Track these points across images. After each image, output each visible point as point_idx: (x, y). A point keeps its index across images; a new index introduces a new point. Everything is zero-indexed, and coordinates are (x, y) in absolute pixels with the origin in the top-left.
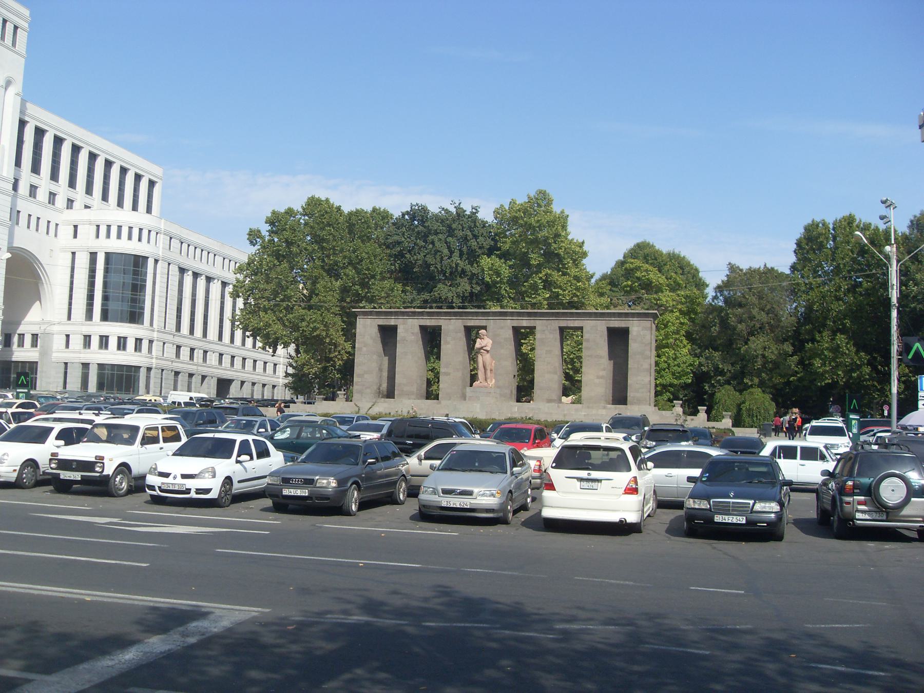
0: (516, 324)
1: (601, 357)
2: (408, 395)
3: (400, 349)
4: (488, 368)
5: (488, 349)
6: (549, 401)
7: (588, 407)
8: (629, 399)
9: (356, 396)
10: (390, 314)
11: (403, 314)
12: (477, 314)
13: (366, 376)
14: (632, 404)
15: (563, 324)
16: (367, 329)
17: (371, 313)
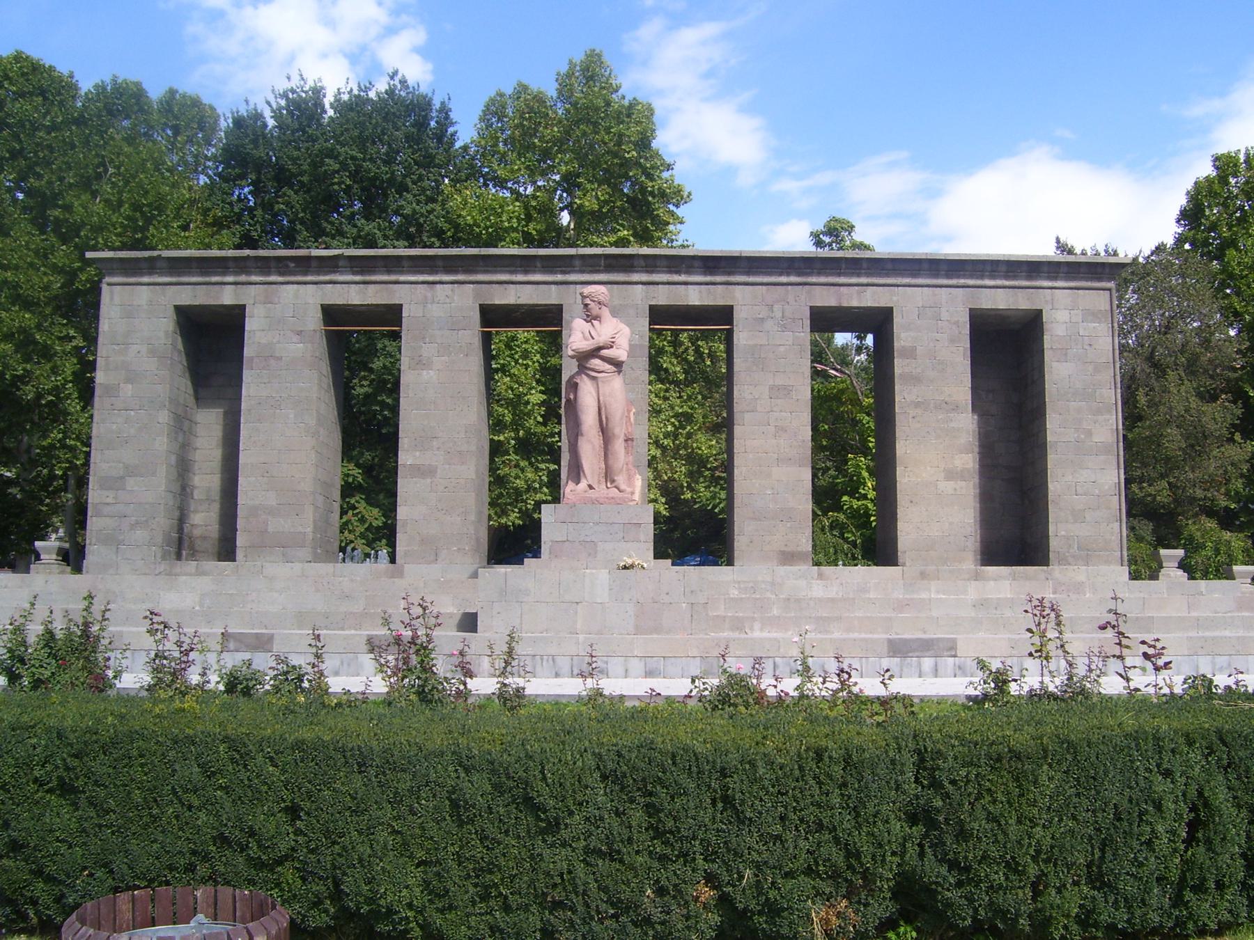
0: (664, 297)
1: (956, 408)
2: (284, 546)
3: (252, 386)
4: (619, 431)
5: (620, 353)
6: (788, 558)
7: (923, 575)
8: (1054, 543)
9: (95, 553)
10: (221, 265)
11: (265, 265)
12: (526, 264)
13: (131, 483)
14: (1063, 561)
15: (827, 298)
16: (136, 323)
17: (151, 266)
